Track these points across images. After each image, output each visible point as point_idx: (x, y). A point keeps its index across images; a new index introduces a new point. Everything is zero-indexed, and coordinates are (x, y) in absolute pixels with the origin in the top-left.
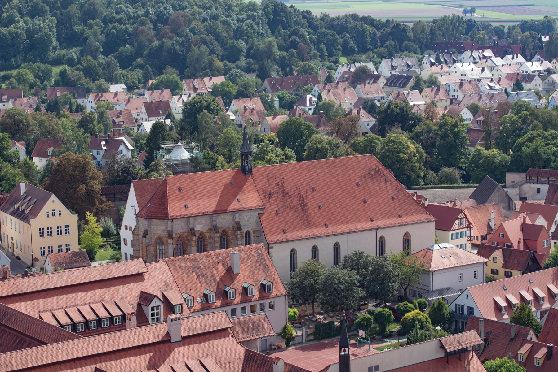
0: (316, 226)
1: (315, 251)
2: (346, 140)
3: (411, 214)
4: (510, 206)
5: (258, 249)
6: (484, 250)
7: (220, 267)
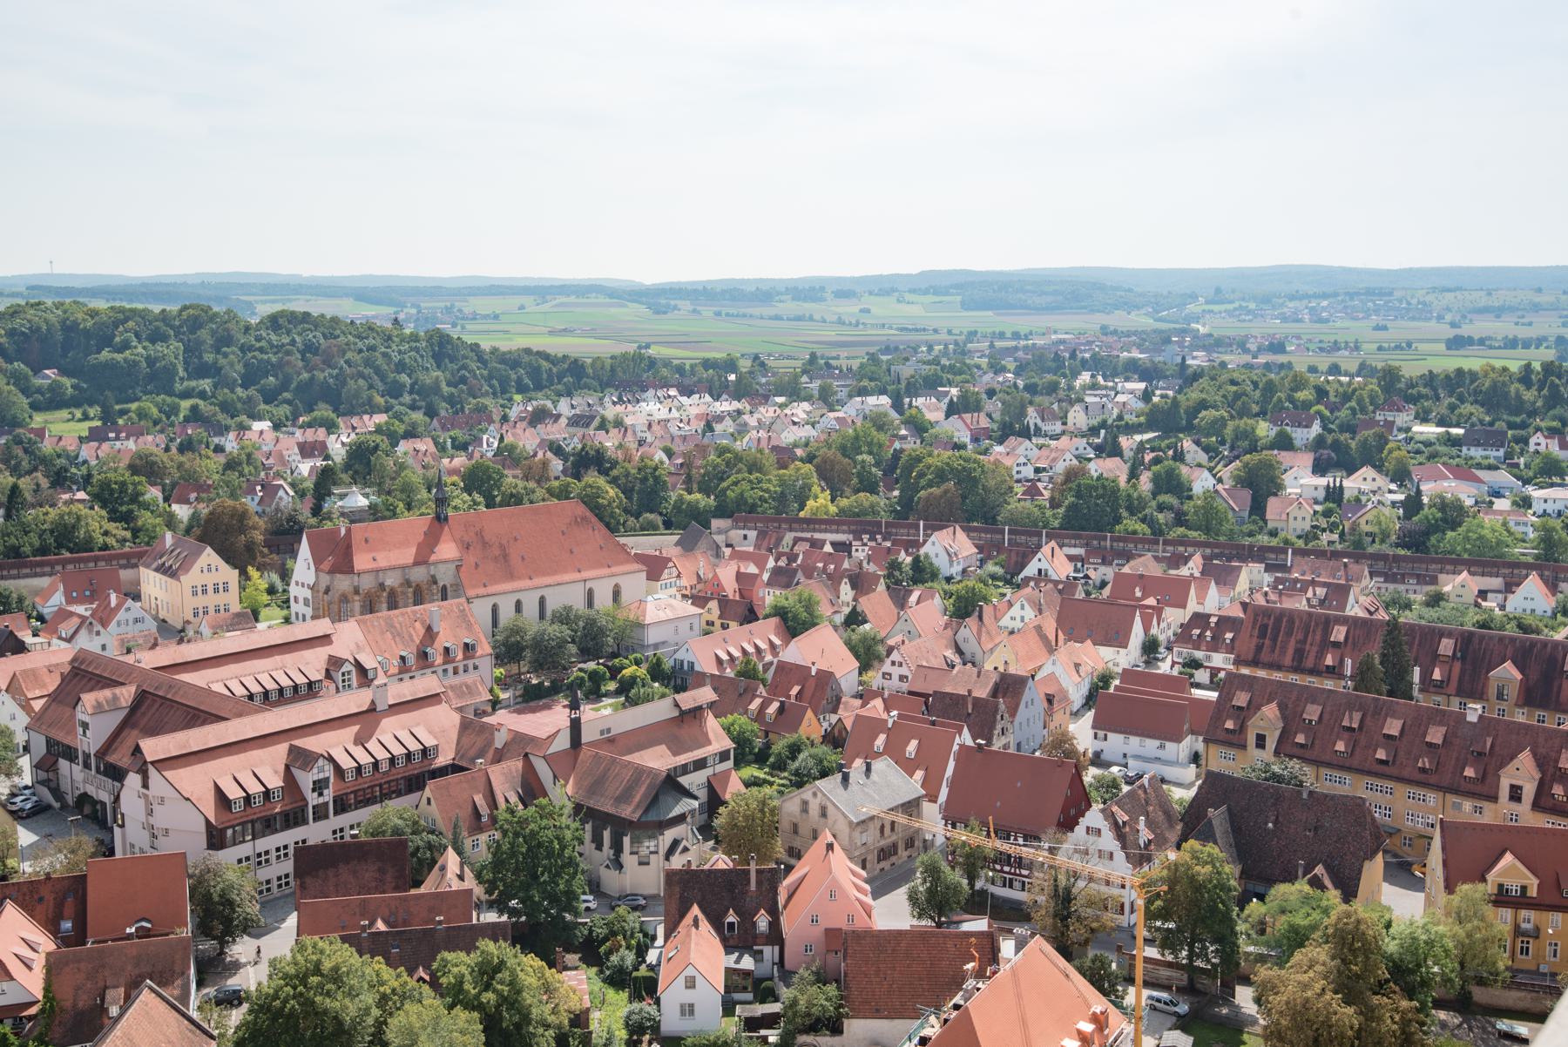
0: (519, 578)
1: (518, 606)
2: (538, 482)
3: (621, 563)
4: (718, 554)
5: (458, 605)
6: (699, 600)
7: (418, 625)
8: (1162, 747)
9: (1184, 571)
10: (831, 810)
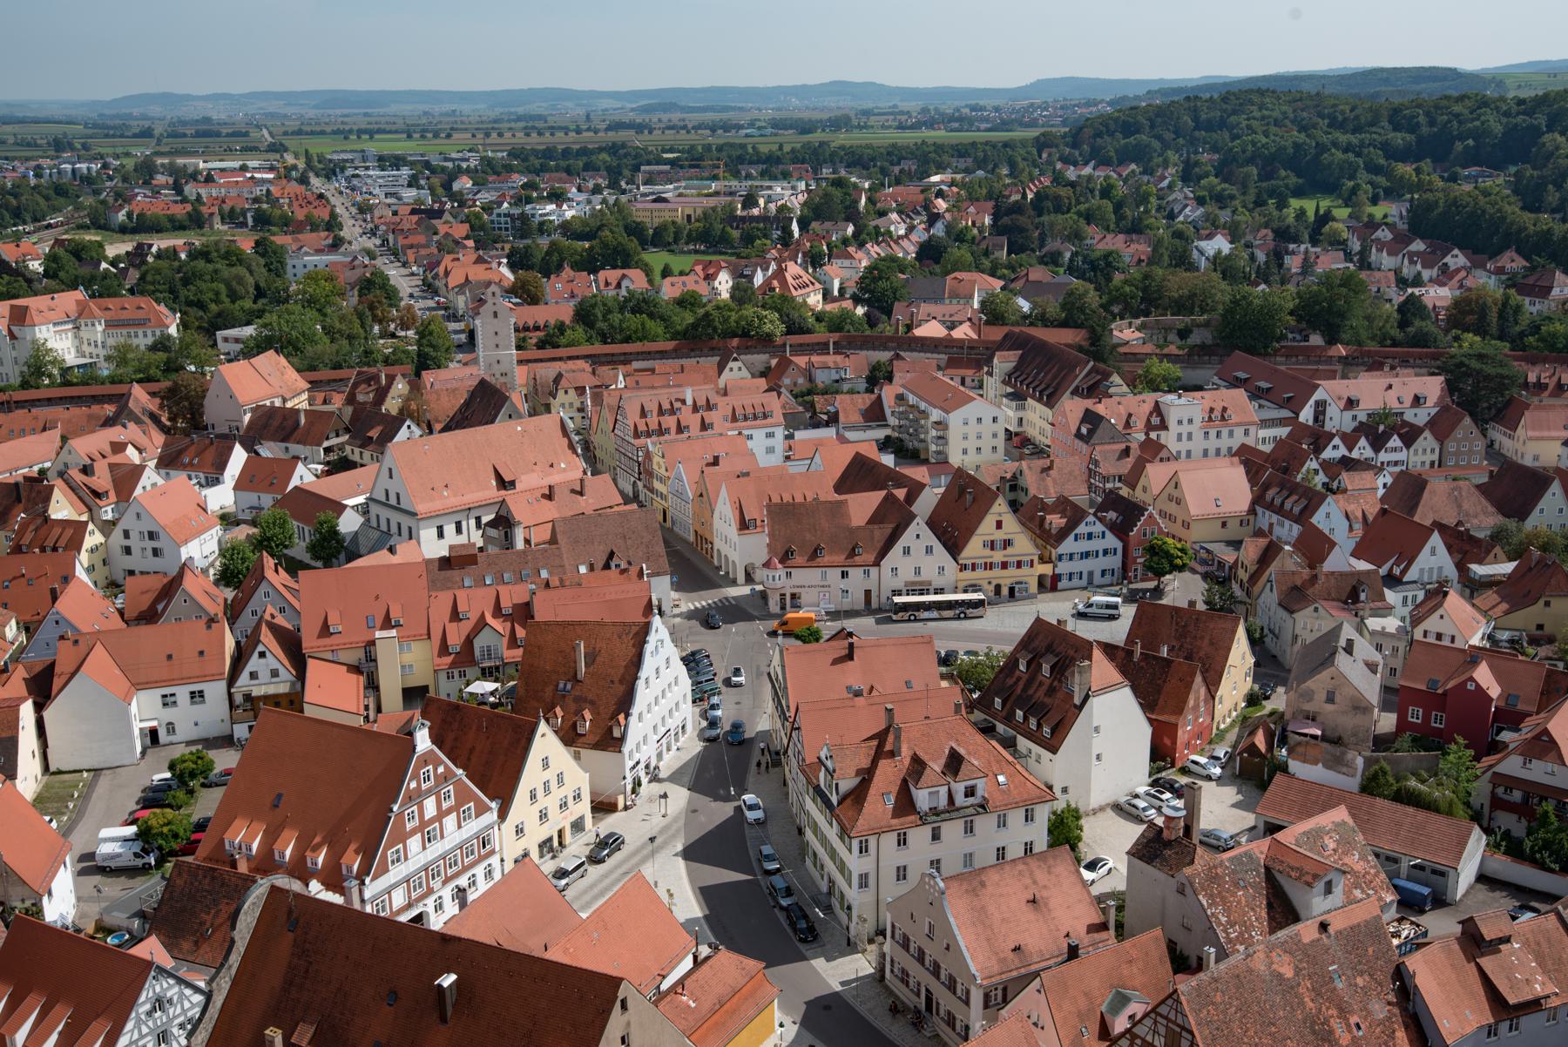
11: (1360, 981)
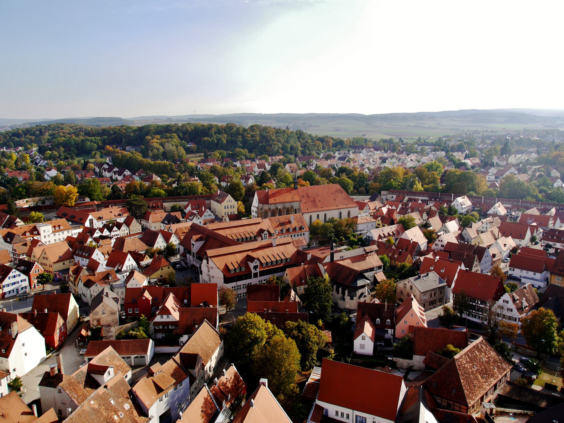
6: (375, 217)
8: (534, 274)
9: (548, 214)
10: (414, 287)
11: (120, 400)
